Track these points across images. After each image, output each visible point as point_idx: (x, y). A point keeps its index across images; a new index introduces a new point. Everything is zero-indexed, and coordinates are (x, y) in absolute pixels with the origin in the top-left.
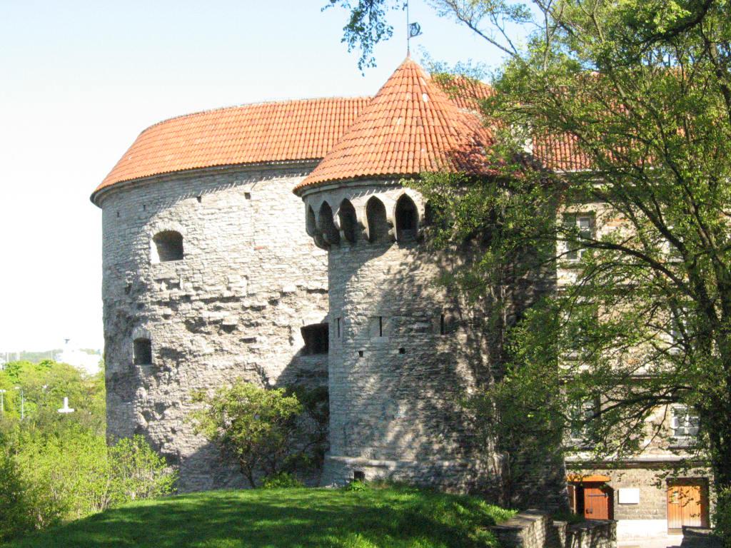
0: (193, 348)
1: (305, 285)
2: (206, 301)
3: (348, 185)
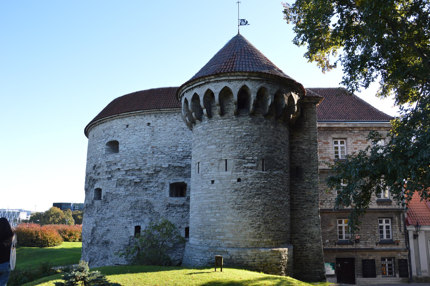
0: (120, 193)
1: (172, 164)
3: (211, 80)
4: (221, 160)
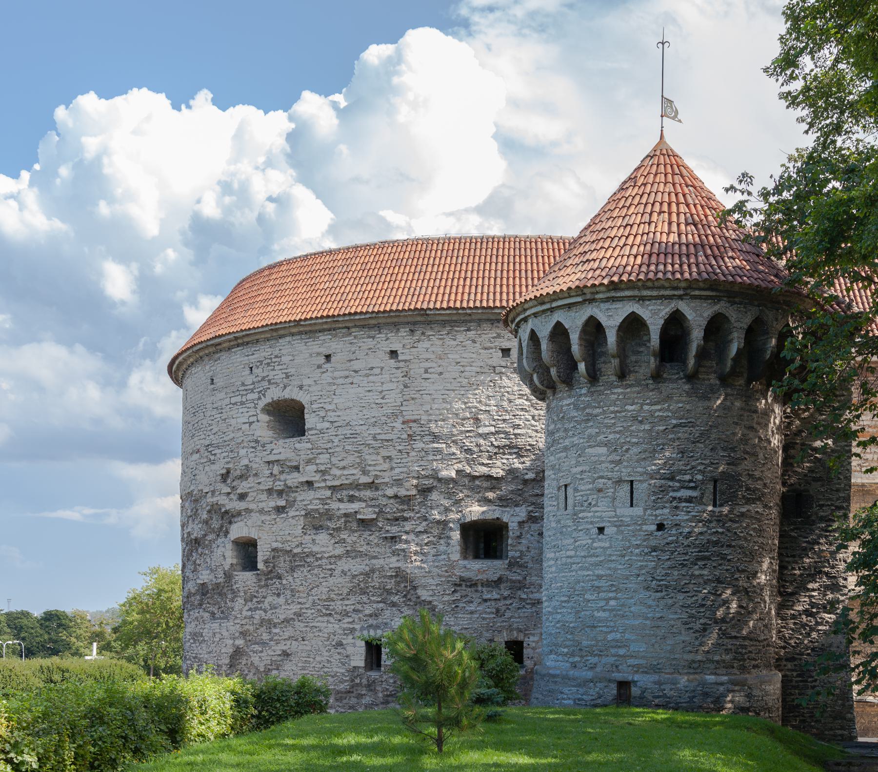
0: (315, 549)
1: (468, 470)
2: (333, 488)
4: (620, 481)
